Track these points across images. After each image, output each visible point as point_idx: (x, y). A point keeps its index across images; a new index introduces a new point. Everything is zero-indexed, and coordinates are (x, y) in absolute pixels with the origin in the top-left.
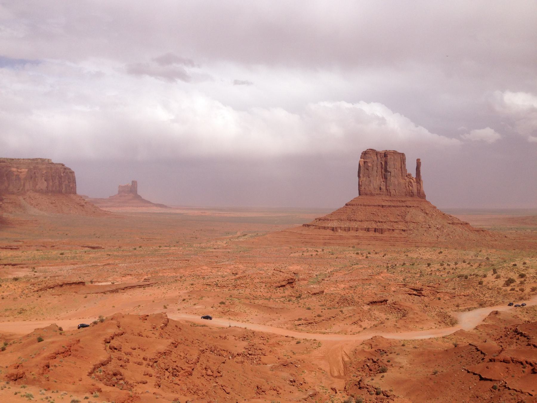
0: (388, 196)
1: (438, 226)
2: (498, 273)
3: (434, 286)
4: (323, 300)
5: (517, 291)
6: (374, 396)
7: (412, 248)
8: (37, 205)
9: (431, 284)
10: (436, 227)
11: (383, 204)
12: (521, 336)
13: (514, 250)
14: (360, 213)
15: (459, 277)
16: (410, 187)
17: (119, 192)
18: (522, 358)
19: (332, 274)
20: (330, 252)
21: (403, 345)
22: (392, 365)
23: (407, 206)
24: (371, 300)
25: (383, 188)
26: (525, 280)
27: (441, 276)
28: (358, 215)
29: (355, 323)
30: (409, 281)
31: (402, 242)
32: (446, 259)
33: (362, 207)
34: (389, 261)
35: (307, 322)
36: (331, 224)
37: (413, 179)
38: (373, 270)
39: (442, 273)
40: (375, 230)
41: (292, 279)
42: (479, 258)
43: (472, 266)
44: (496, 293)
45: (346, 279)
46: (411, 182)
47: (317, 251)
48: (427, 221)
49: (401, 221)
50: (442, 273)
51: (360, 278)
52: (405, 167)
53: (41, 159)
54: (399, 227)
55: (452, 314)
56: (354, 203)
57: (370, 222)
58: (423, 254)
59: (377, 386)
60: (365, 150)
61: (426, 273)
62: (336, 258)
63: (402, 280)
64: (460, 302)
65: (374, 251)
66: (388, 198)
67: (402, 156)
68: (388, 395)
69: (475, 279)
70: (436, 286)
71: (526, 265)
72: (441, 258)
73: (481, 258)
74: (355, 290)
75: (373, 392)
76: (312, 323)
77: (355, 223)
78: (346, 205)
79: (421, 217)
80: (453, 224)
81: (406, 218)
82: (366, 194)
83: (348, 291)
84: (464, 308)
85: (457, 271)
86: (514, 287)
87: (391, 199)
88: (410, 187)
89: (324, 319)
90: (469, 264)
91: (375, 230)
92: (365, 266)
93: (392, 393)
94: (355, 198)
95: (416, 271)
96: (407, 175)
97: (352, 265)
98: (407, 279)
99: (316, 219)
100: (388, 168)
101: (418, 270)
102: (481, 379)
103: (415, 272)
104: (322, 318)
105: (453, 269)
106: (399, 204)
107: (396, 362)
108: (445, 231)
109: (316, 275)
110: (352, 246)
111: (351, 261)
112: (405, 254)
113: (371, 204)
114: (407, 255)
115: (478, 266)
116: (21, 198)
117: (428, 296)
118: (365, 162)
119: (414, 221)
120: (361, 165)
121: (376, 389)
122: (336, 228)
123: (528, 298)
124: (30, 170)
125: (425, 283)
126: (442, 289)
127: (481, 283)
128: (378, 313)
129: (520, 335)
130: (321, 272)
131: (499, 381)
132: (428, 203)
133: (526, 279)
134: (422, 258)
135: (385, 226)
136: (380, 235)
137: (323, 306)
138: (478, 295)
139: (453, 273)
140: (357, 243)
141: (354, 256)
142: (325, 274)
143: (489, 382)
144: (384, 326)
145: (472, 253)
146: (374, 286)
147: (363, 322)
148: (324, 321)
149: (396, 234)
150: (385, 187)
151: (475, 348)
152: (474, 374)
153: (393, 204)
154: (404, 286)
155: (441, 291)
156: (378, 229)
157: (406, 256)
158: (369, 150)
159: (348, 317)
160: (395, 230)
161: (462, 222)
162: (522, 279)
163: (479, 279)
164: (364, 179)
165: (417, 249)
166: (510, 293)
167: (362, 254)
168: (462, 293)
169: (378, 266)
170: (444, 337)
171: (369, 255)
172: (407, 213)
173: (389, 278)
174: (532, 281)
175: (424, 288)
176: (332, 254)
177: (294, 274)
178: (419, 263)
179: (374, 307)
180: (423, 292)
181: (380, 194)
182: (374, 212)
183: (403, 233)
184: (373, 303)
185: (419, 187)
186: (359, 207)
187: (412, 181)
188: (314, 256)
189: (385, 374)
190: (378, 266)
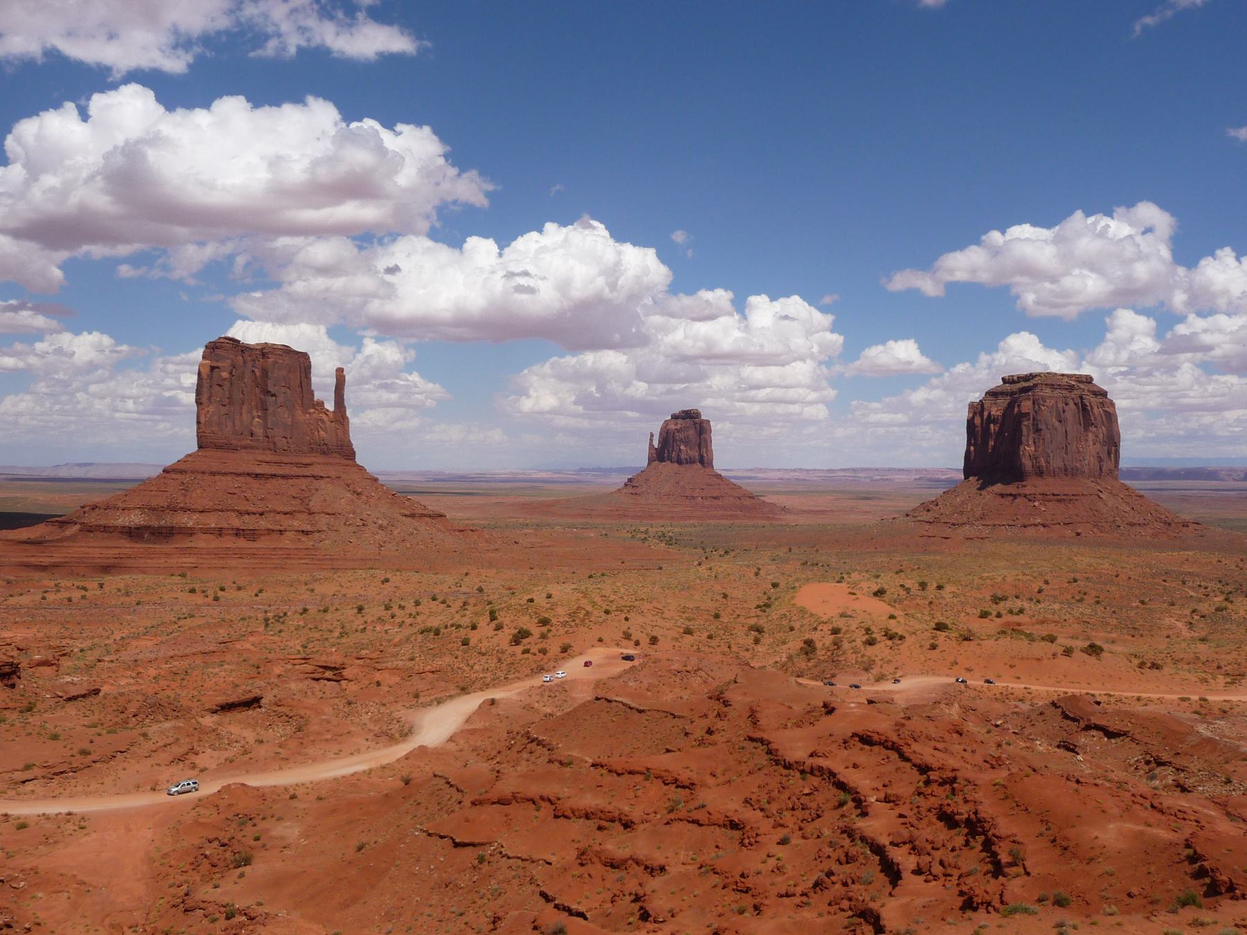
0: (269, 452)
1: (380, 522)
2: (500, 619)
3: (370, 657)
4: (96, 713)
5: (535, 655)
6: (222, 923)
7: (323, 574)
9: (364, 652)
10: (376, 526)
11: (258, 470)
12: (538, 745)
13: (532, 568)
14: (198, 491)
15: (422, 633)
16: (322, 432)
18: (534, 790)
19: (123, 643)
20: (119, 590)
21: (293, 797)
22: (264, 846)
23: (314, 476)
24: (221, 699)
25: (259, 431)
26: (549, 631)
27: (386, 632)
28: (194, 495)
29: (180, 759)
30: (314, 650)
31: (301, 559)
32: (397, 594)
33: (206, 477)
34: (270, 606)
35: (49, 770)
36: (123, 520)
37: (326, 414)
38: (231, 629)
39: (387, 627)
40: (238, 533)
41: (11, 664)
42: (464, 589)
43: (449, 606)
44: (495, 661)
45: (161, 655)
46: (322, 421)
47: (85, 589)
48: (358, 511)
49: (300, 512)
50: (387, 627)
51: (199, 649)
54: (295, 524)
55: (401, 712)
56: (182, 467)
57: (225, 514)
58: (349, 584)
59: (226, 900)
60: (214, 339)
61: (353, 629)
62: (138, 604)
63: (299, 648)
64: (421, 686)
65: (234, 583)
67: (301, 360)
68: (253, 915)
69: (453, 636)
70: (374, 655)
71: (551, 600)
72: (386, 592)
73: (468, 590)
74: (183, 679)
75: (218, 915)
76: (62, 773)
77: (186, 516)
79: (342, 499)
80: (412, 516)
81: (311, 504)
83: (163, 683)
84: (429, 699)
85: (419, 619)
86: (528, 647)
88: (322, 432)
89: (96, 759)
90: (444, 602)
91: (238, 533)
92: (211, 620)
93: (261, 910)
94: (189, 455)
95: (332, 624)
97: (179, 619)
98: (311, 645)
99: (83, 507)
100: (269, 385)
101: (336, 623)
102: (456, 845)
103: (329, 627)
104: (93, 757)
105: (410, 615)
106: (295, 471)
107: (271, 838)
108: (396, 532)
109: (82, 651)
110: (180, 572)
111: (175, 608)
112: (307, 587)
113: (227, 470)
114: (312, 590)
115: (461, 607)
117: (356, 679)
118: (213, 368)
119: (330, 511)
120: (205, 376)
121: (224, 907)
122: (138, 529)
123: (554, 667)
125: (351, 650)
126: (388, 662)
127: (465, 643)
128: (238, 727)
129: (535, 743)
130: (96, 641)
131: (490, 844)
132: (361, 469)
133: (552, 628)
134: (345, 595)
135: (263, 523)
136: (251, 545)
137: (96, 727)
138: (459, 668)
139: (411, 625)
140: (189, 565)
141: (185, 597)
142: (106, 645)
143: (471, 848)
144: (251, 759)
145: (450, 579)
146: (231, 667)
147: (201, 755)
148: (98, 765)
149: (287, 542)
151: (444, 781)
152: (442, 837)
153: (281, 472)
154: (303, 661)
155: (384, 665)
156: (243, 530)
157: (309, 593)
158: (222, 340)
159: (160, 747)
161: (431, 513)
162: (544, 629)
163: (462, 632)
164: (211, 409)
165: (335, 576)
166: (520, 660)
167: (203, 592)
168: (428, 668)
169: (242, 619)
170: (384, 768)
171: (220, 594)
172: (313, 491)
173: (268, 646)
174: (562, 631)
175: (348, 661)
176: (127, 594)
177: (18, 649)
178: (339, 607)
179: (229, 716)
180: (345, 673)
181: (251, 447)
182: (235, 491)
183: (304, 539)
184: (227, 708)
186: (199, 477)
187: (324, 417)
188: (74, 600)
189: (247, 869)
190: (242, 619)
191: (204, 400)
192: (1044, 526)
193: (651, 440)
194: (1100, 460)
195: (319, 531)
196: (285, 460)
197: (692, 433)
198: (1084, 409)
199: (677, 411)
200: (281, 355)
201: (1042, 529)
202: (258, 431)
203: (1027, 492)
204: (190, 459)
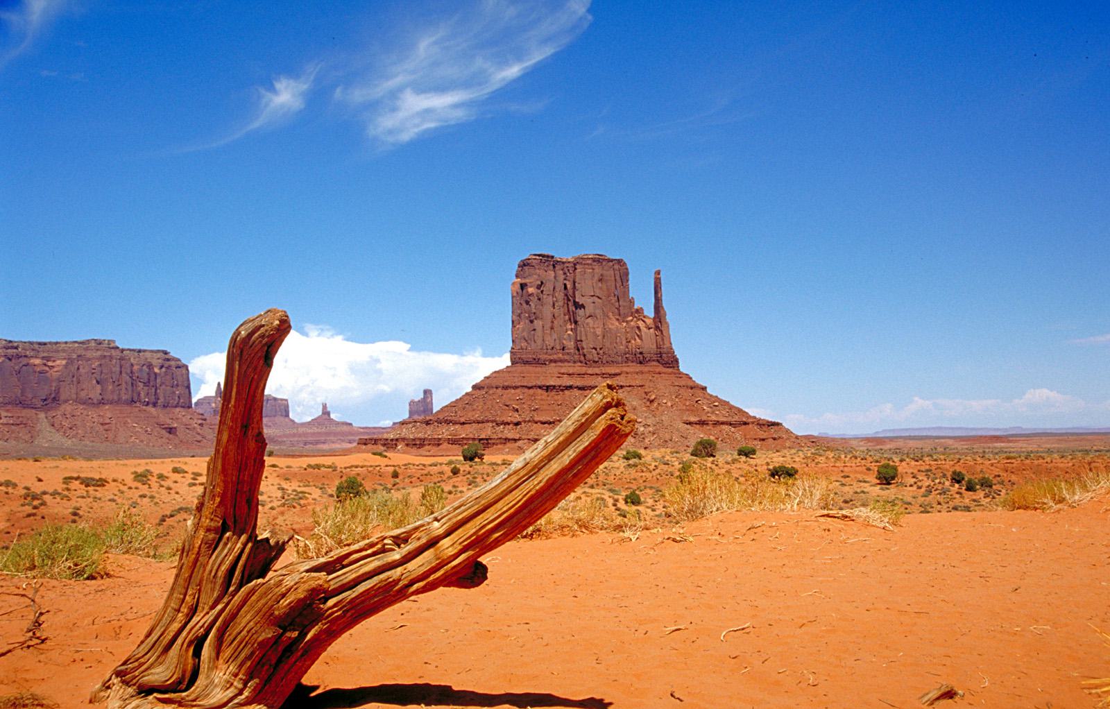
8: (71, 429)
16: (638, 340)
17: (411, 413)
25: (570, 345)
37: (644, 321)
46: (638, 328)
52: (626, 292)
53: (96, 340)
66: (578, 368)
67: (616, 267)
78: (475, 387)
82: (526, 363)
87: (584, 370)
96: (632, 313)
116: (42, 415)
118: (523, 286)
124: (70, 361)
150: (572, 343)
160: (519, 440)
181: (561, 361)
185: (659, 339)
187: (641, 324)
196: (590, 371)
200: (591, 264)
202: (569, 344)
204: (497, 375)
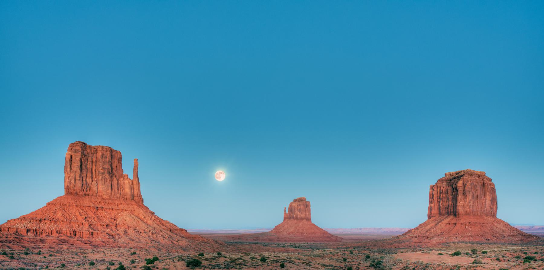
94: (59, 197)
191: (69, 170)
192: (472, 236)
193: (285, 211)
194: (491, 208)
195: (119, 235)
197: (302, 207)
198: (484, 184)
199: (296, 199)
201: (471, 238)
203: (462, 222)
